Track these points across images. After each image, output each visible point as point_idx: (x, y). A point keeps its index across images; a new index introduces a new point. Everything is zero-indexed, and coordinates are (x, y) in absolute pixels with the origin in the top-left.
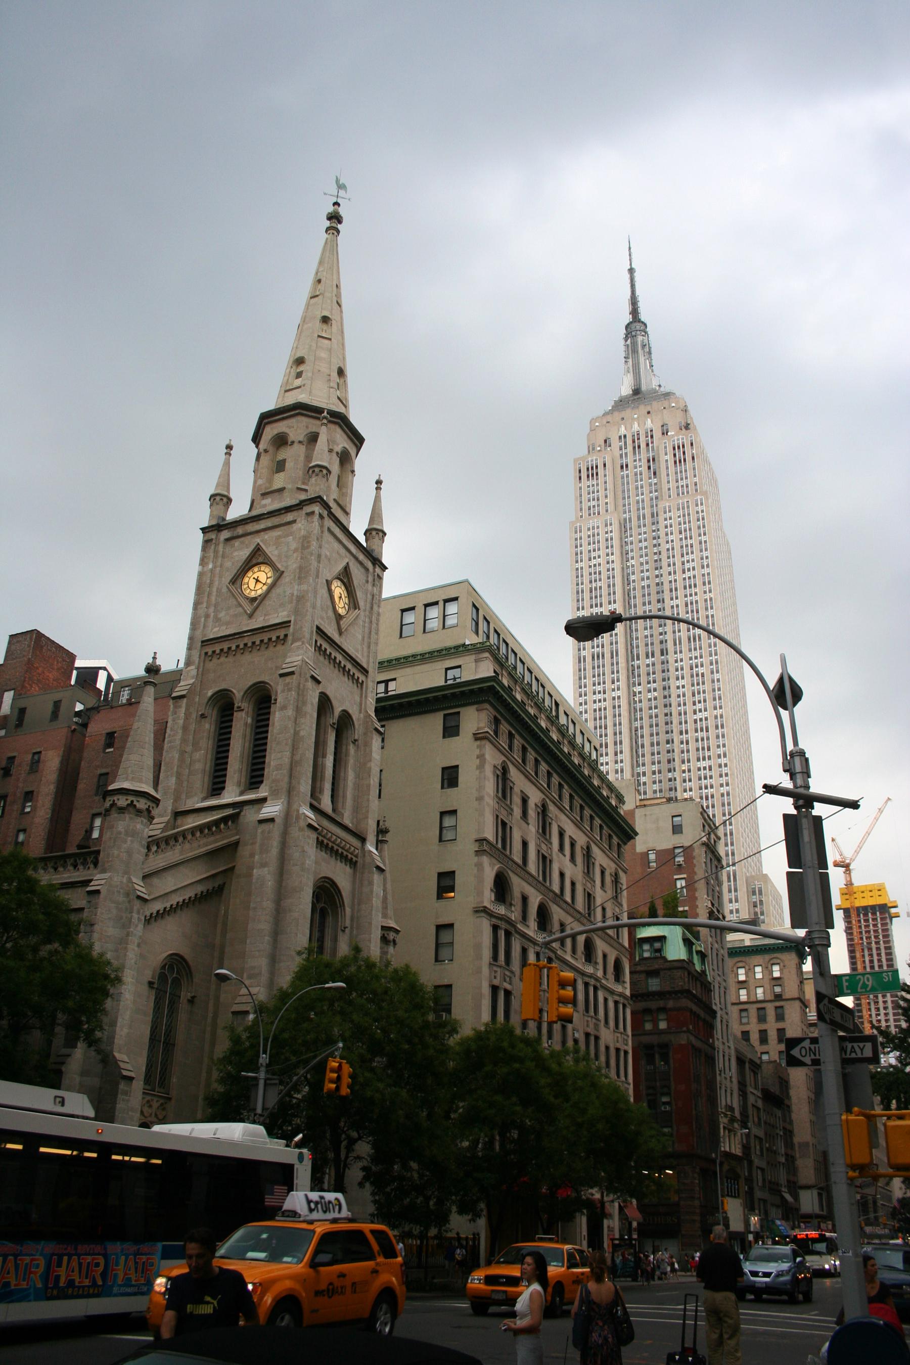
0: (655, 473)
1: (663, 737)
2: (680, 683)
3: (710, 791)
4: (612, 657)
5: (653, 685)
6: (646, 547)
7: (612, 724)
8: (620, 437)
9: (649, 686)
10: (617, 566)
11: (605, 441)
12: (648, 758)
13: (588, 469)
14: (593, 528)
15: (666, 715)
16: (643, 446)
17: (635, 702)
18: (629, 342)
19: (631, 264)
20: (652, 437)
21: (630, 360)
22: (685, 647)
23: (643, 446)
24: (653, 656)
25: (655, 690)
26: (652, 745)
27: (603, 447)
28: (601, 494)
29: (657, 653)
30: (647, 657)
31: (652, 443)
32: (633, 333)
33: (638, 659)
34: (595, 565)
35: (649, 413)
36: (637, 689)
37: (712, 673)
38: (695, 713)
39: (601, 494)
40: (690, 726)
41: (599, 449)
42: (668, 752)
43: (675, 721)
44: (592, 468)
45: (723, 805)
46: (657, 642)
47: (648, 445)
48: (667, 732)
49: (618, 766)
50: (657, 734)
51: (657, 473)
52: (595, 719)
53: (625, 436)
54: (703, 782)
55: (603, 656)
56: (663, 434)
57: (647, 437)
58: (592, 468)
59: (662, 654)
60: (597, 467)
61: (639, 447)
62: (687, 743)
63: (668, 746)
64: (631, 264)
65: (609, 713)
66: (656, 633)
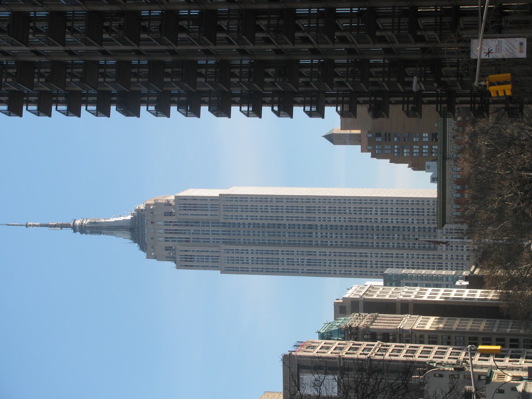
0: (197, 223)
1: (359, 232)
2: (332, 219)
3: (394, 210)
4: (311, 255)
5: (329, 235)
6: (244, 232)
7: (349, 257)
8: (166, 241)
9: (328, 237)
10: (255, 248)
11: (166, 250)
12: (370, 241)
14: (228, 260)
15: (346, 229)
16: (176, 228)
17: (337, 245)
18: (89, 231)
19: (24, 225)
20: (171, 222)
21: (103, 231)
22: (313, 215)
24: (312, 233)
25: (331, 234)
26: (362, 238)
27: (170, 251)
28: (205, 254)
29: (310, 231)
30: (312, 236)
31: (175, 222)
33: (312, 241)
34: (252, 261)
35: (152, 223)
36: (329, 243)
37: (330, 202)
38: (351, 213)
39: (205, 254)
40: (357, 216)
42: (368, 229)
43: (354, 224)
45: (402, 204)
46: (303, 231)
47: (176, 225)
48: (357, 229)
49: (374, 255)
50: (357, 234)
51: (197, 221)
52: (345, 266)
53: (166, 238)
54: (389, 212)
55: (309, 260)
57: (170, 225)
58: (186, 258)
59: (312, 228)
61: (176, 230)
62: (366, 219)
63: (364, 229)
64: (24, 225)
65: (343, 258)
66: (298, 230)
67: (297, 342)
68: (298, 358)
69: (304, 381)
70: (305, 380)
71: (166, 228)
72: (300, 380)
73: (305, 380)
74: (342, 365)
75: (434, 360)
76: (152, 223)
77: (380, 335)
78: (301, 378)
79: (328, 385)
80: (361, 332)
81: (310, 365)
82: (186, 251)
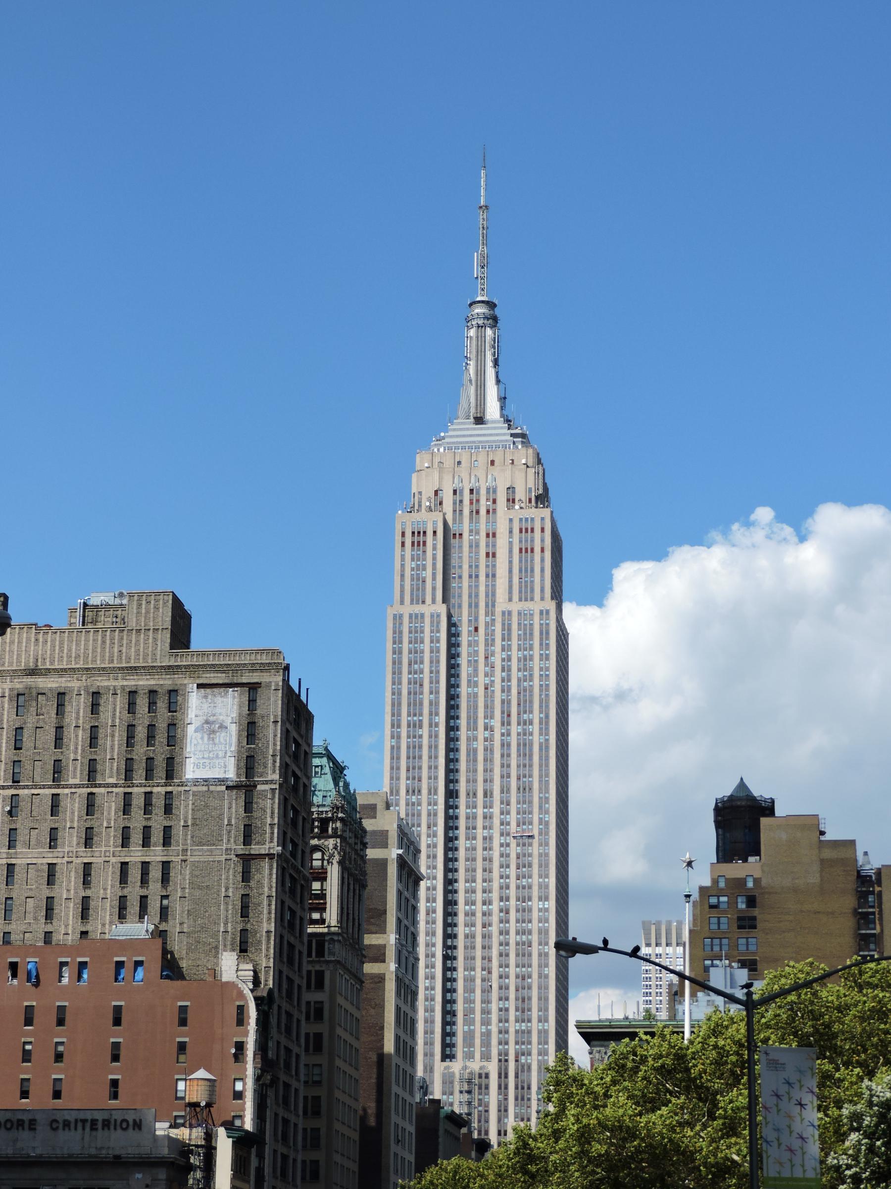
8: (455, 492)
11: (436, 493)
13: (413, 533)
16: (483, 512)
20: (494, 501)
23: (483, 512)
27: (433, 500)
29: (480, 794)
32: (481, 322)
41: (428, 504)
44: (419, 533)
47: (488, 512)
56: (508, 500)
57: (487, 500)
58: (419, 533)
60: (425, 533)
61: (478, 512)
67: (307, 689)
68: (273, 684)
69: (219, 700)
70: (223, 702)
71: (483, 492)
72: (222, 690)
73: (223, 702)
74: (259, 787)
75: (275, 1007)
76: (492, 463)
77: (322, 890)
78: (228, 692)
79: (211, 755)
80: (326, 843)
81: (258, 712)
82: (435, 532)
